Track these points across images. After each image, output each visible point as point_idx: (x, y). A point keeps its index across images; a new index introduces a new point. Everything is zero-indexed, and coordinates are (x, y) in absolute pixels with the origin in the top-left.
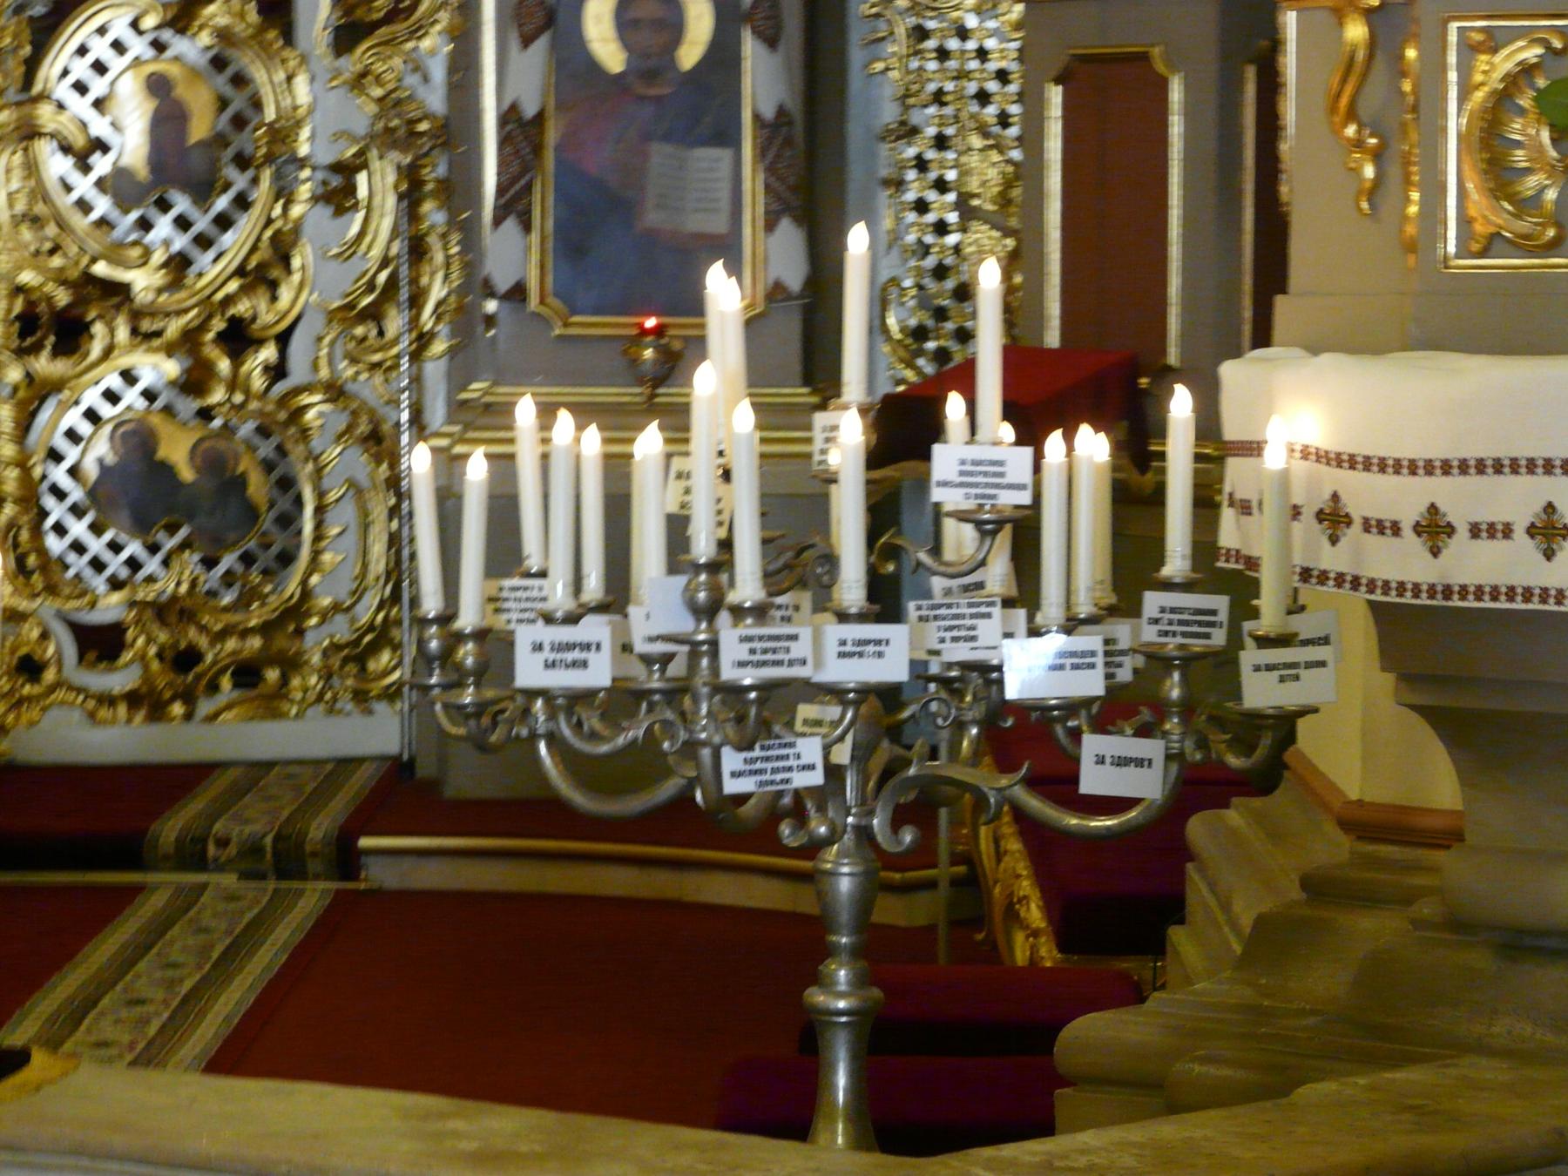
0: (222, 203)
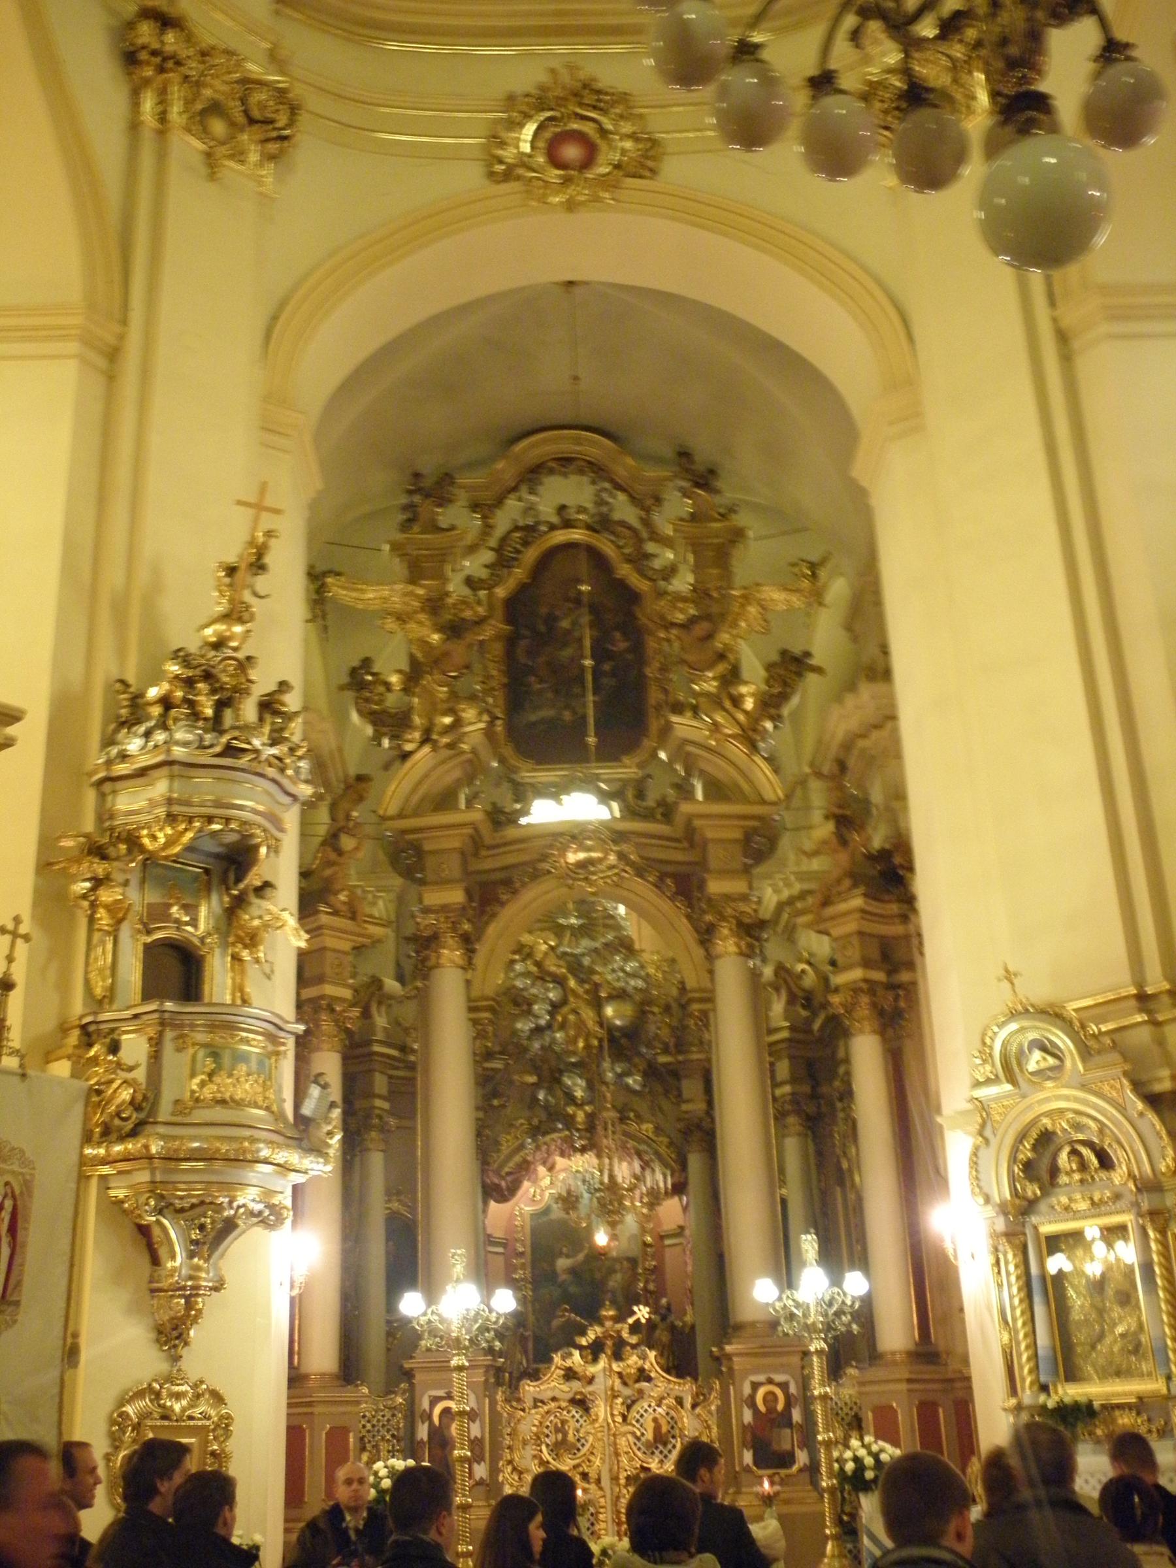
0: (670, 1446)
